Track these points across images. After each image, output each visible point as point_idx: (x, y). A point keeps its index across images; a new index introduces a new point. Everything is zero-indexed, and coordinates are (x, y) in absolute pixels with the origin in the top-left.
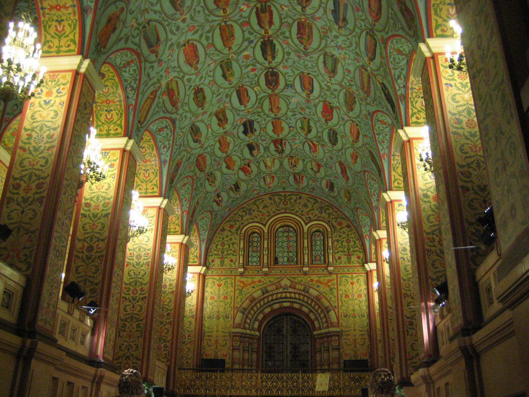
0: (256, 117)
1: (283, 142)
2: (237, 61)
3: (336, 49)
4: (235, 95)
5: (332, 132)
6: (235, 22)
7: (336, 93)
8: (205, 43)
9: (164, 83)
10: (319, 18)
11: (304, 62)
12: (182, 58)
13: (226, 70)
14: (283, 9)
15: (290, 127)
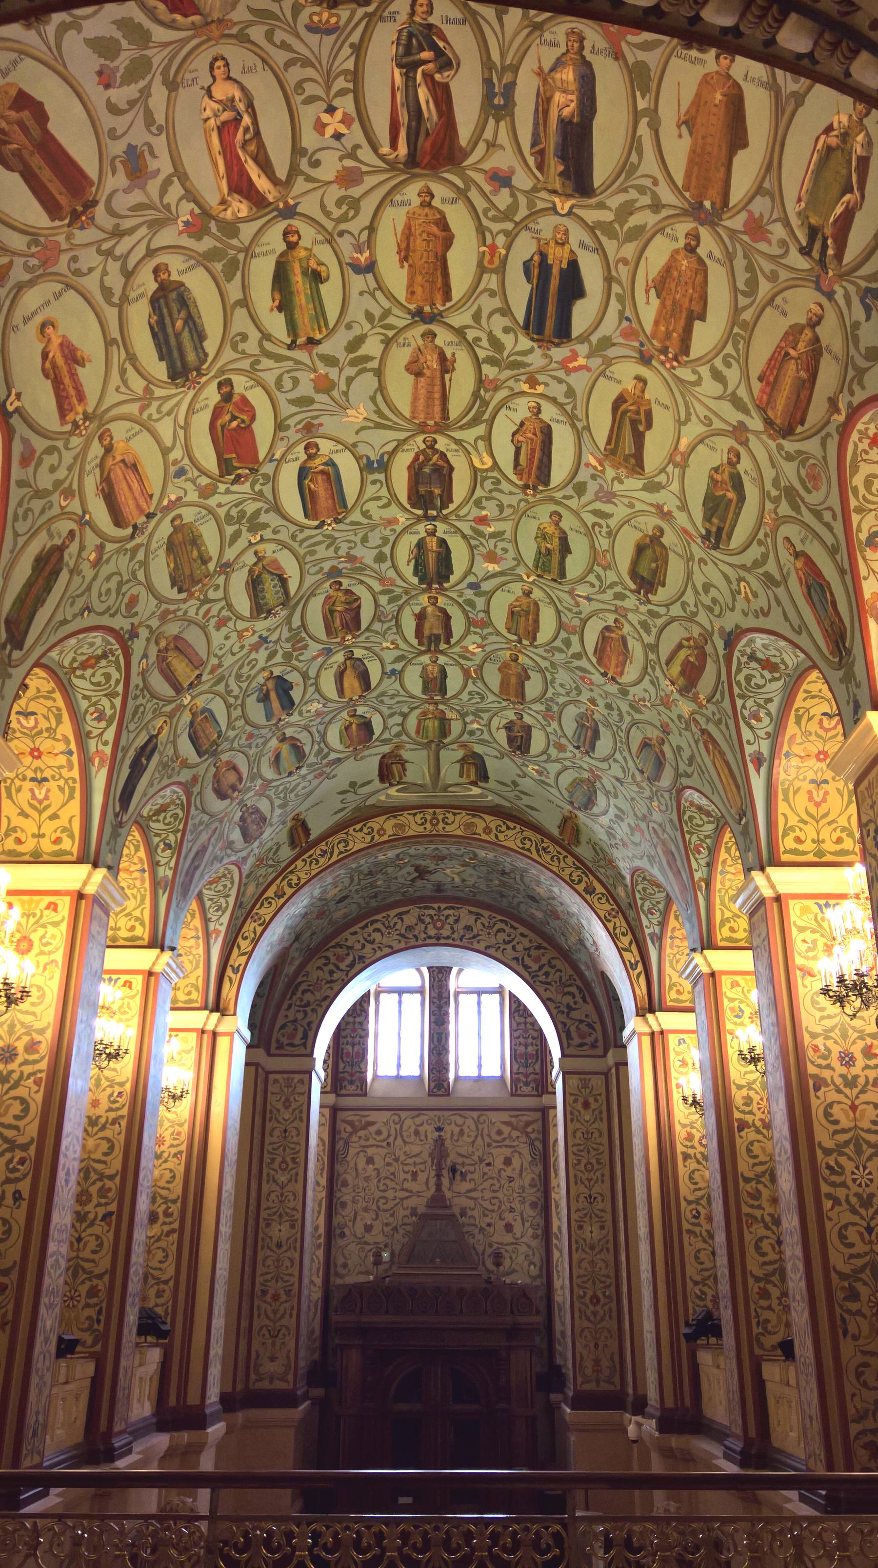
0: (507, 340)
1: (403, 149)
2: (519, 559)
3: (265, 634)
4: (558, 475)
5: (191, 357)
6: (498, 633)
7: (230, 530)
8: (575, 639)
10: (315, 658)
11: (337, 550)
13: (556, 558)
14: (393, 643)
15: (370, 267)
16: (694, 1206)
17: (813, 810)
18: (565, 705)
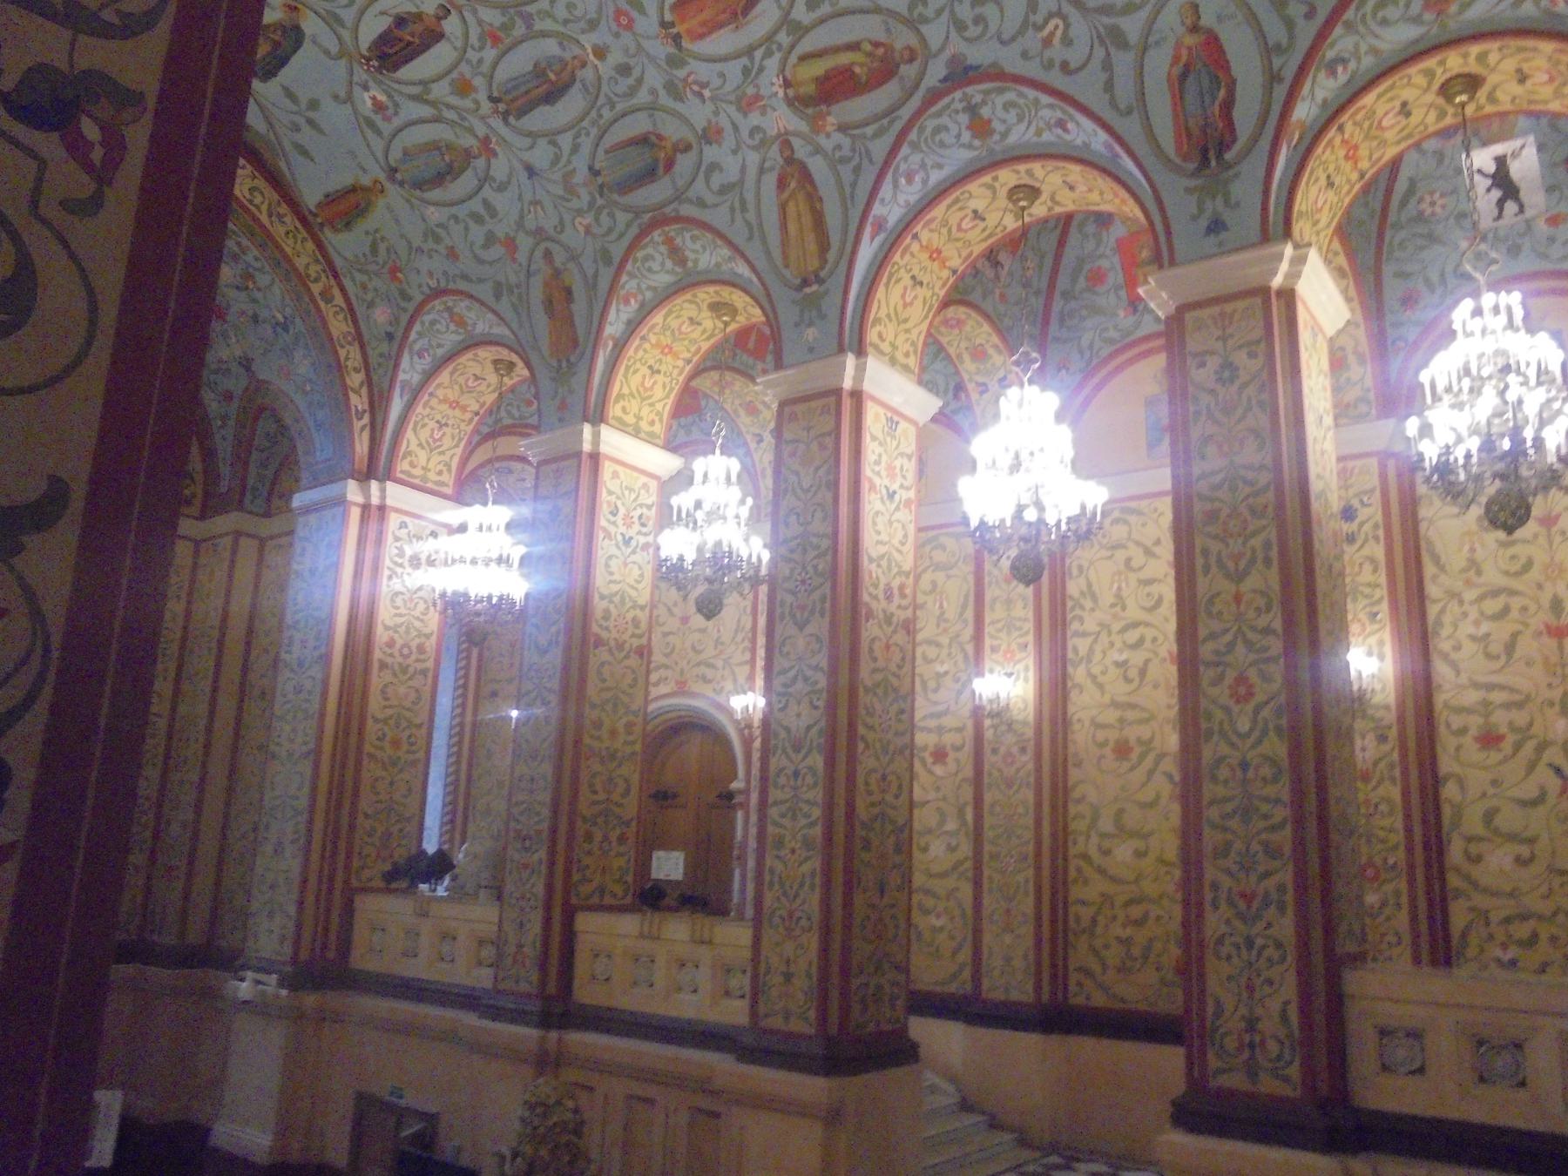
9: (782, 119)
12: (723, 41)
16: (379, 726)
17: (900, 308)
18: (544, 34)
